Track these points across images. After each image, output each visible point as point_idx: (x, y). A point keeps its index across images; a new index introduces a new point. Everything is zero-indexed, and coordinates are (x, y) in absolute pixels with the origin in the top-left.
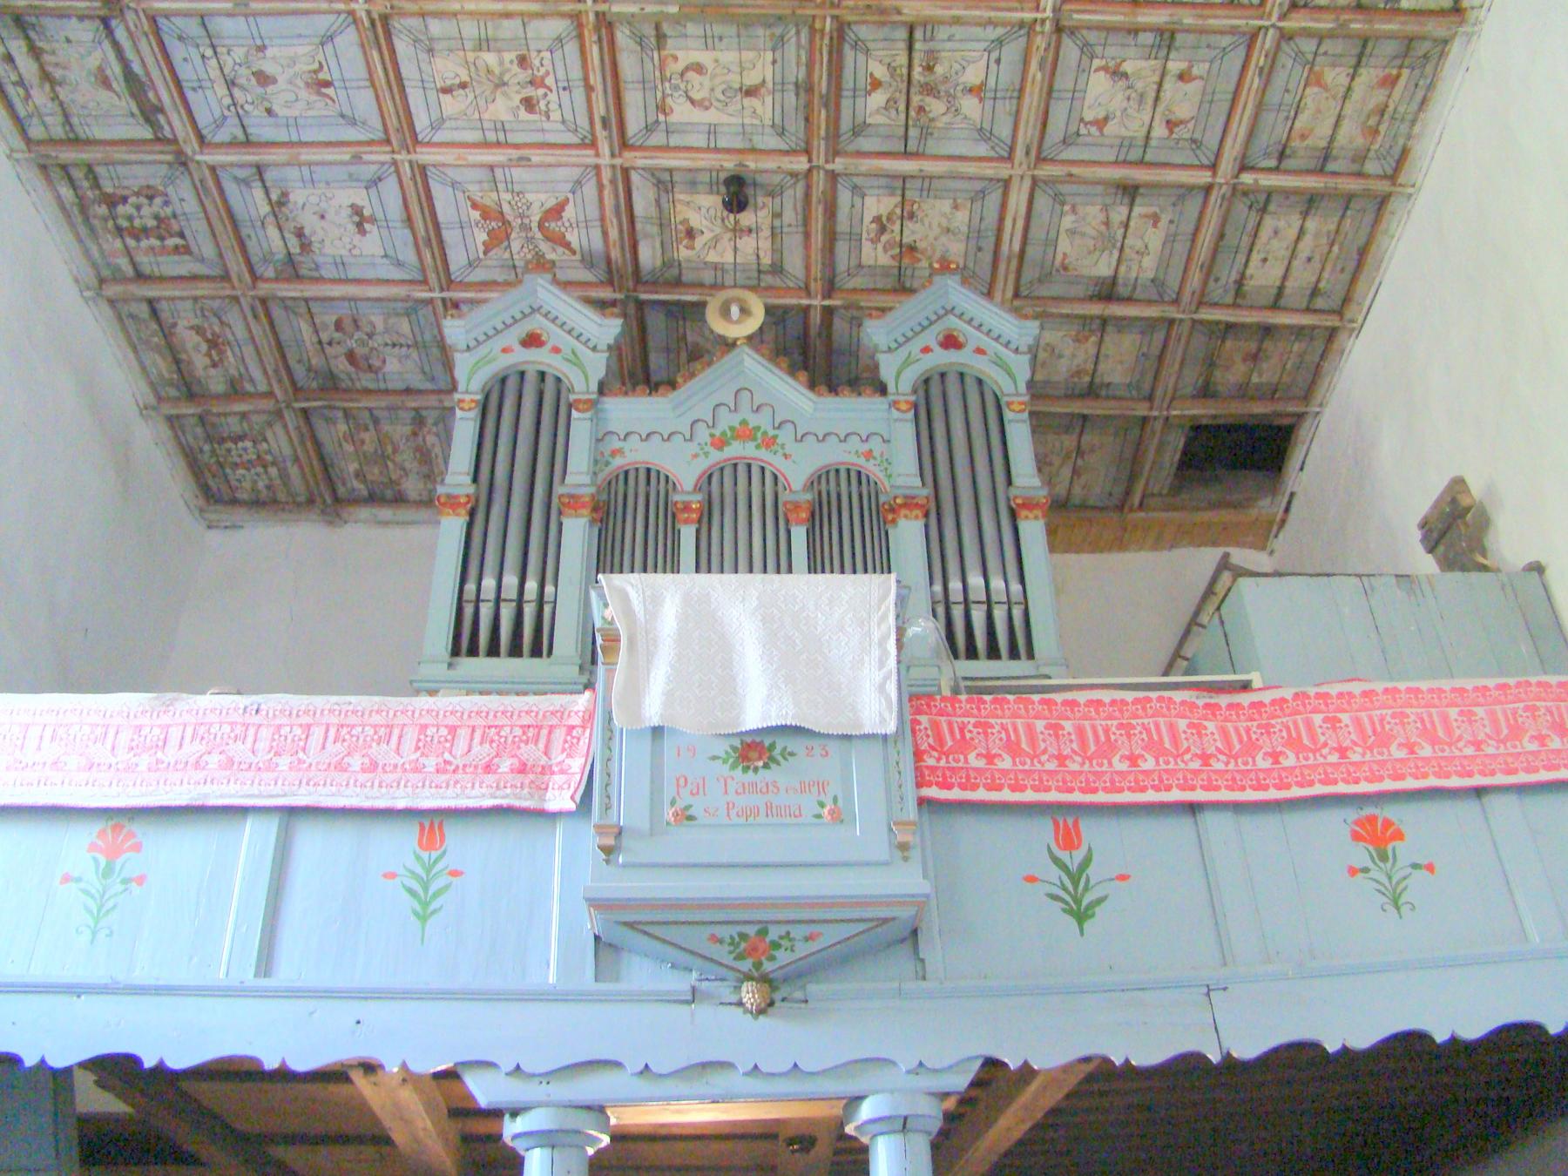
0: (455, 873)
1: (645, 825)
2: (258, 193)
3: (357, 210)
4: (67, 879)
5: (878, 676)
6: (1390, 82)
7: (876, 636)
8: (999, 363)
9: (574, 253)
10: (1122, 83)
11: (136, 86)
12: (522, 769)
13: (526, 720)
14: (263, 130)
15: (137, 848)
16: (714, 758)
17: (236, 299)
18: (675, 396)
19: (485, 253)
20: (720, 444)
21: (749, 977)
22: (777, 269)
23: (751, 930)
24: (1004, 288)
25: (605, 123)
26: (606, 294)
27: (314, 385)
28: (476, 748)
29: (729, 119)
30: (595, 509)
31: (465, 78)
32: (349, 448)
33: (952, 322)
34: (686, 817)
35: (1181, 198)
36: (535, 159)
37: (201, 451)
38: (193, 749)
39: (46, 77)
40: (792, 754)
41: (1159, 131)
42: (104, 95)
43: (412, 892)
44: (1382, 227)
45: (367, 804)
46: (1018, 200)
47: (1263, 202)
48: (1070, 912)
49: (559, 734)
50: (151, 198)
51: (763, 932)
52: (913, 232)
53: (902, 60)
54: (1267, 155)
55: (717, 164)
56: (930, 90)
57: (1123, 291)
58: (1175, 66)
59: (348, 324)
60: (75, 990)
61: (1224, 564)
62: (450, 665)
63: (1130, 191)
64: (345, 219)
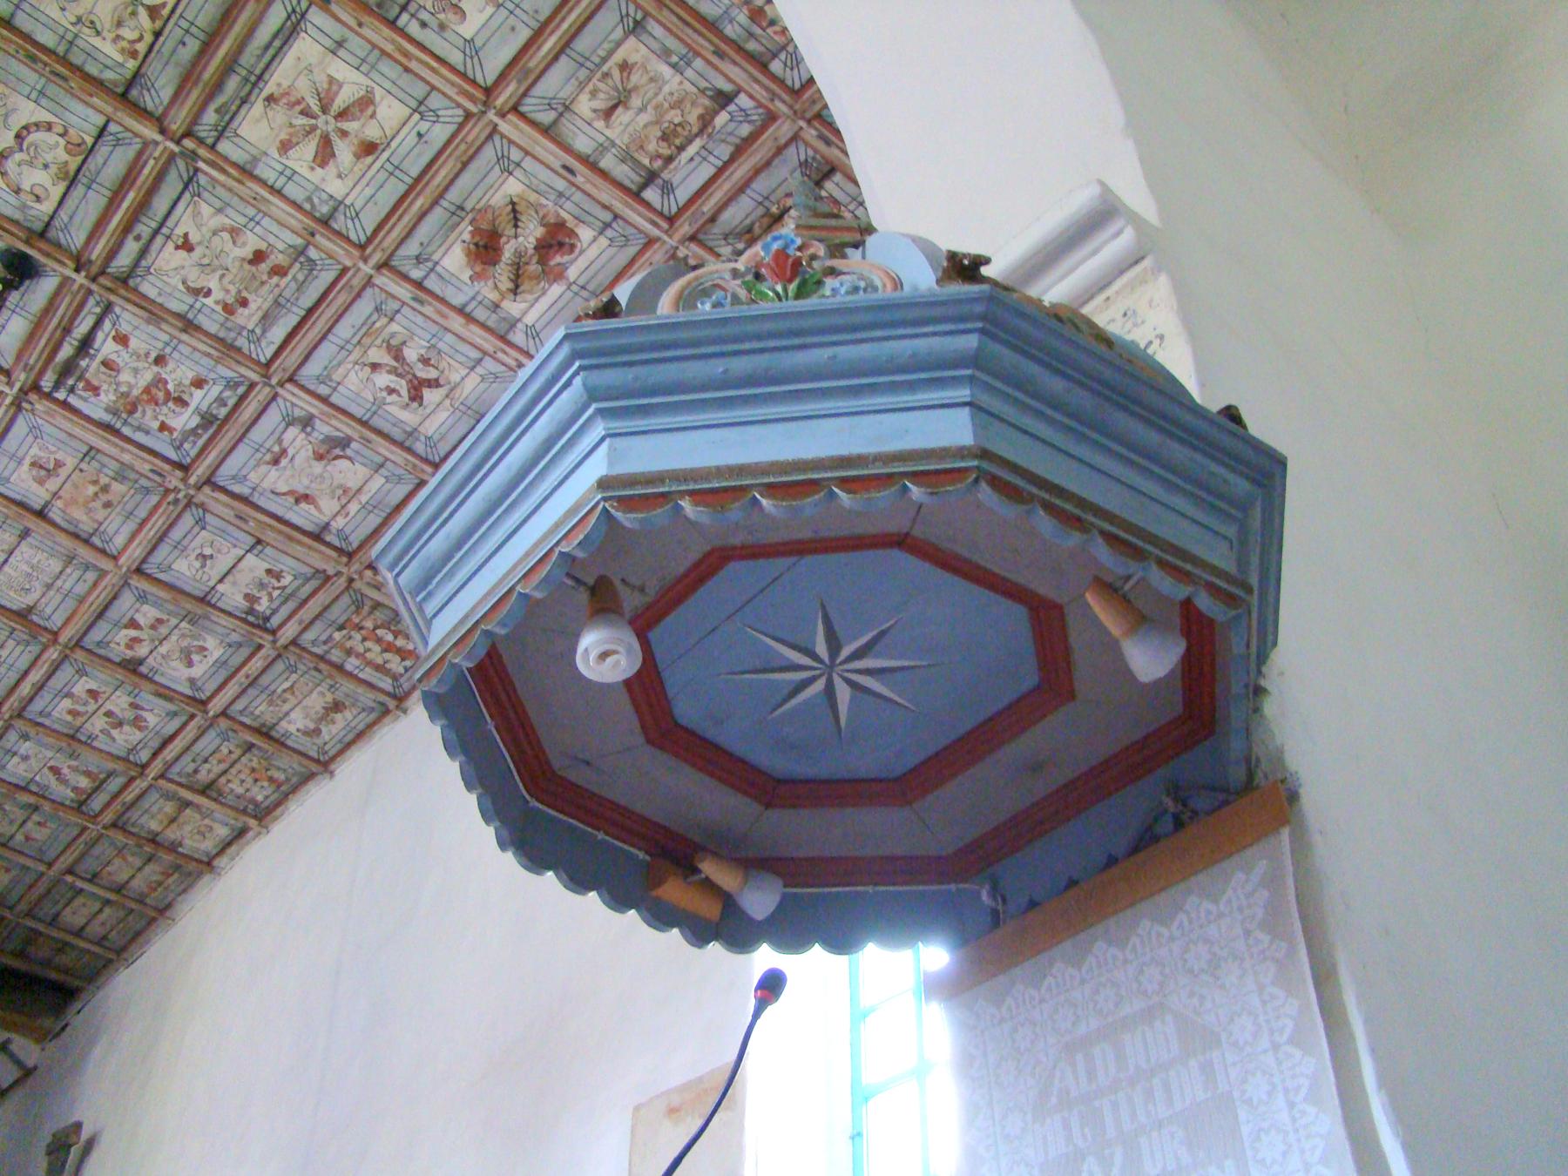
41: (19, 837)
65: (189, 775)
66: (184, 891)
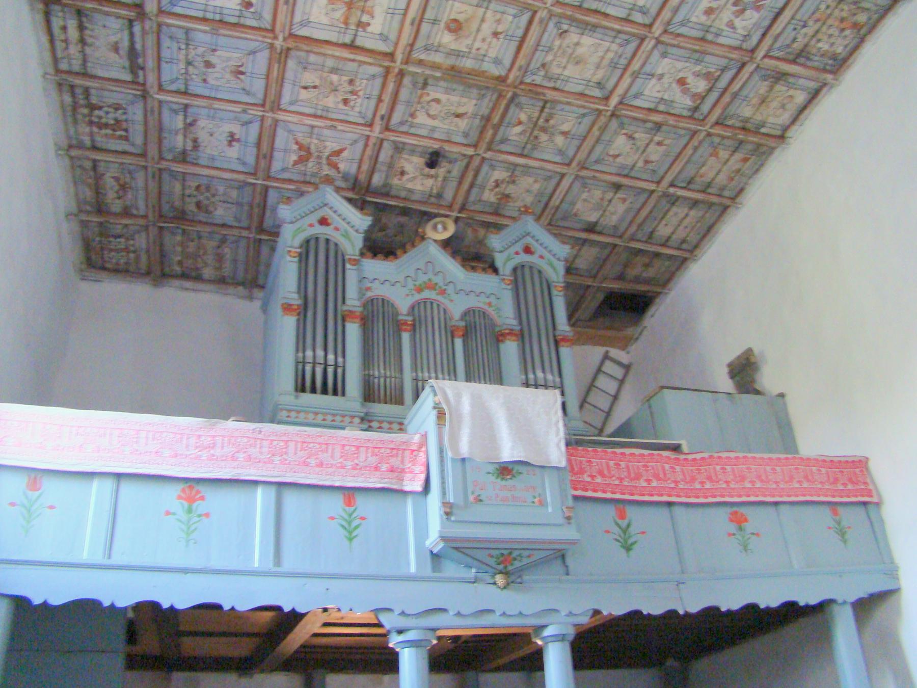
0: (363, 518)
1: (461, 502)
2: (181, 117)
3: (232, 135)
4: (168, 513)
5: (556, 440)
6: (745, 160)
7: (554, 420)
8: (551, 264)
9: (339, 172)
10: (631, 142)
11: (133, 53)
12: (392, 470)
13: (392, 446)
14: (197, 87)
15: (202, 498)
16: (489, 473)
17: (145, 168)
18: (397, 261)
19: (294, 165)
20: (419, 290)
21: (501, 572)
22: (439, 196)
23: (505, 552)
24: (545, 220)
25: (382, 118)
26: (350, 195)
27: (171, 215)
28: (370, 459)
29: (442, 127)
30: (362, 319)
31: (317, 84)
32: (179, 249)
33: (529, 240)
34: (479, 500)
35: (639, 193)
36: (340, 128)
37: (94, 240)
38: (230, 450)
39: (82, 41)
40: (520, 473)
41: (640, 164)
42: (113, 56)
43: (343, 526)
44: (722, 219)
45: (321, 483)
46: (566, 183)
47: (674, 201)
48: (622, 546)
49: (407, 453)
50: (116, 109)
51: (510, 553)
52: (510, 189)
53: (536, 115)
54: (682, 181)
55: (429, 145)
56: (544, 130)
57: (598, 228)
58: (657, 139)
59: (203, 188)
60: (185, 571)
61: (606, 357)
62: (297, 397)
63: (617, 187)
64: (224, 138)
65: (788, 46)
66: (757, 171)
